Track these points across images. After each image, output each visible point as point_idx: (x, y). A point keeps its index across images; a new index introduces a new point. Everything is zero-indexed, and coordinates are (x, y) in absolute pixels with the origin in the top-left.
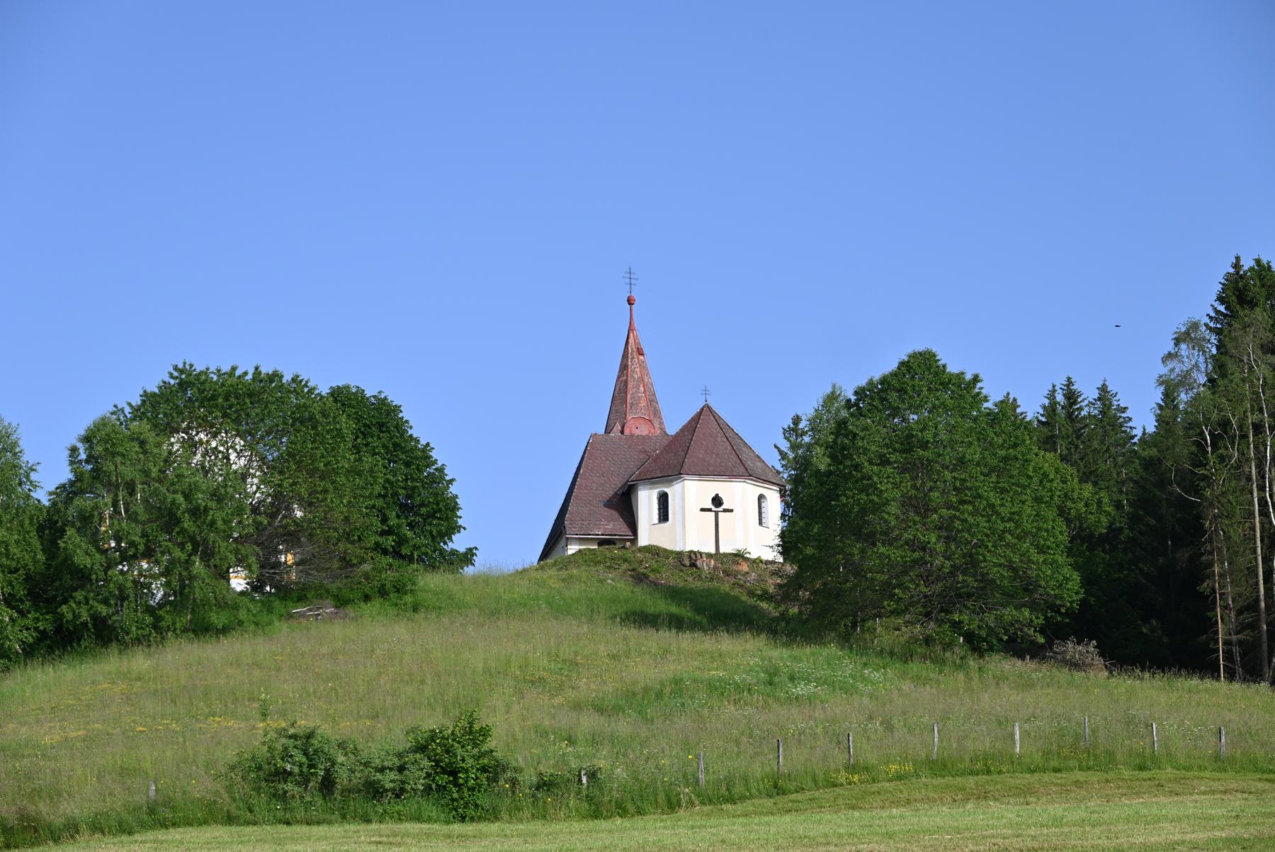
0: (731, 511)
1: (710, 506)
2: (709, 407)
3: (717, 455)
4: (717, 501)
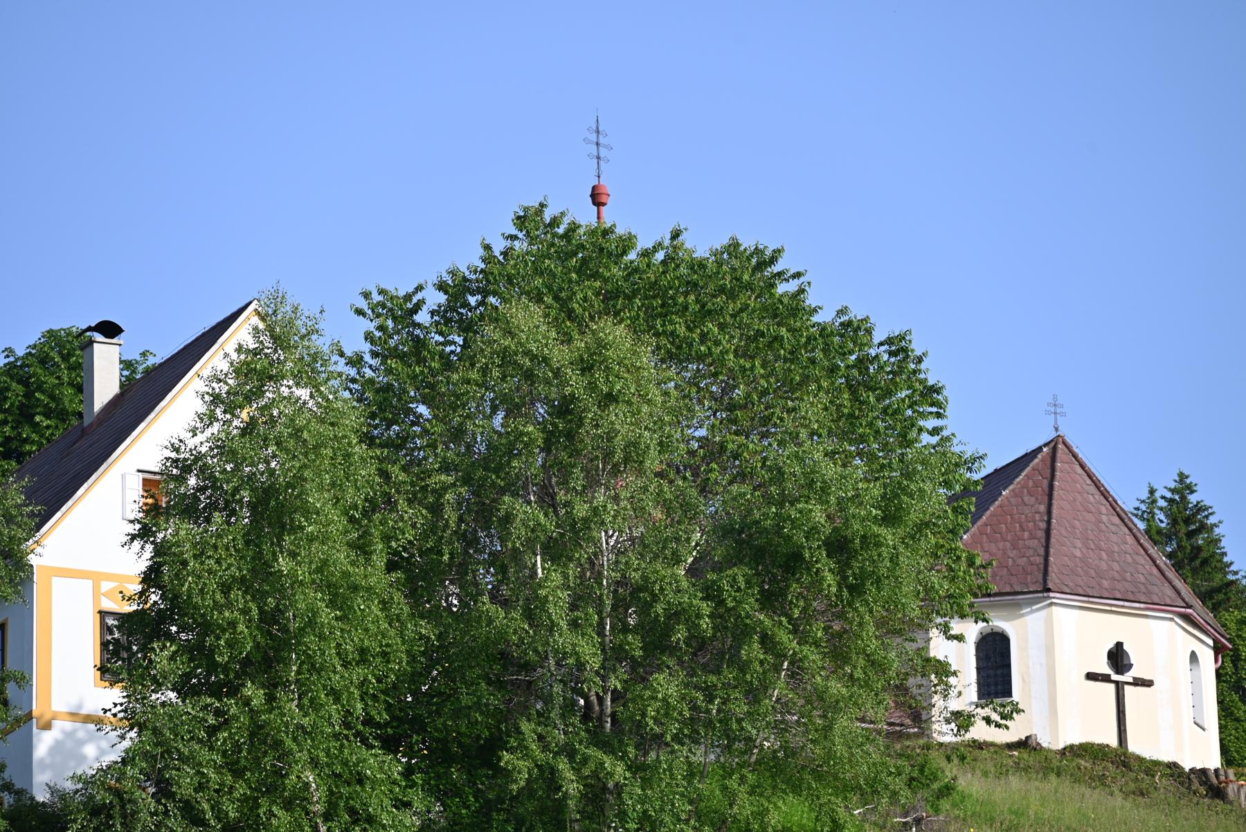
0: (1148, 683)
1: (1105, 669)
2: (1064, 443)
3: (1110, 553)
4: (1118, 657)
